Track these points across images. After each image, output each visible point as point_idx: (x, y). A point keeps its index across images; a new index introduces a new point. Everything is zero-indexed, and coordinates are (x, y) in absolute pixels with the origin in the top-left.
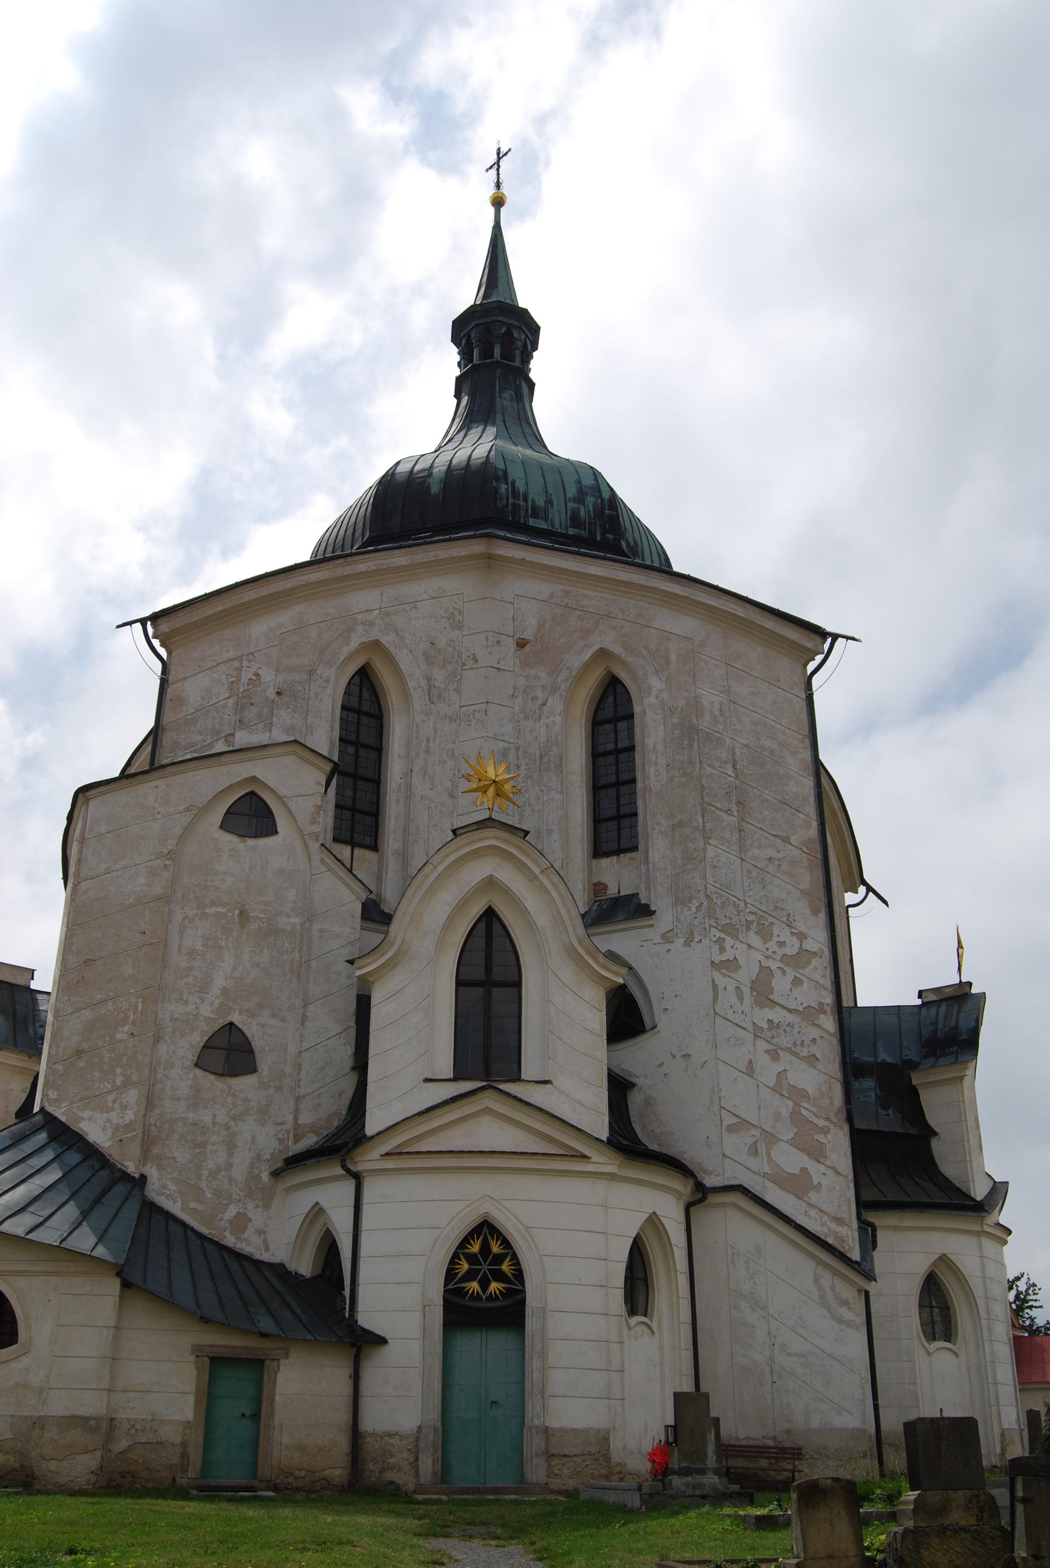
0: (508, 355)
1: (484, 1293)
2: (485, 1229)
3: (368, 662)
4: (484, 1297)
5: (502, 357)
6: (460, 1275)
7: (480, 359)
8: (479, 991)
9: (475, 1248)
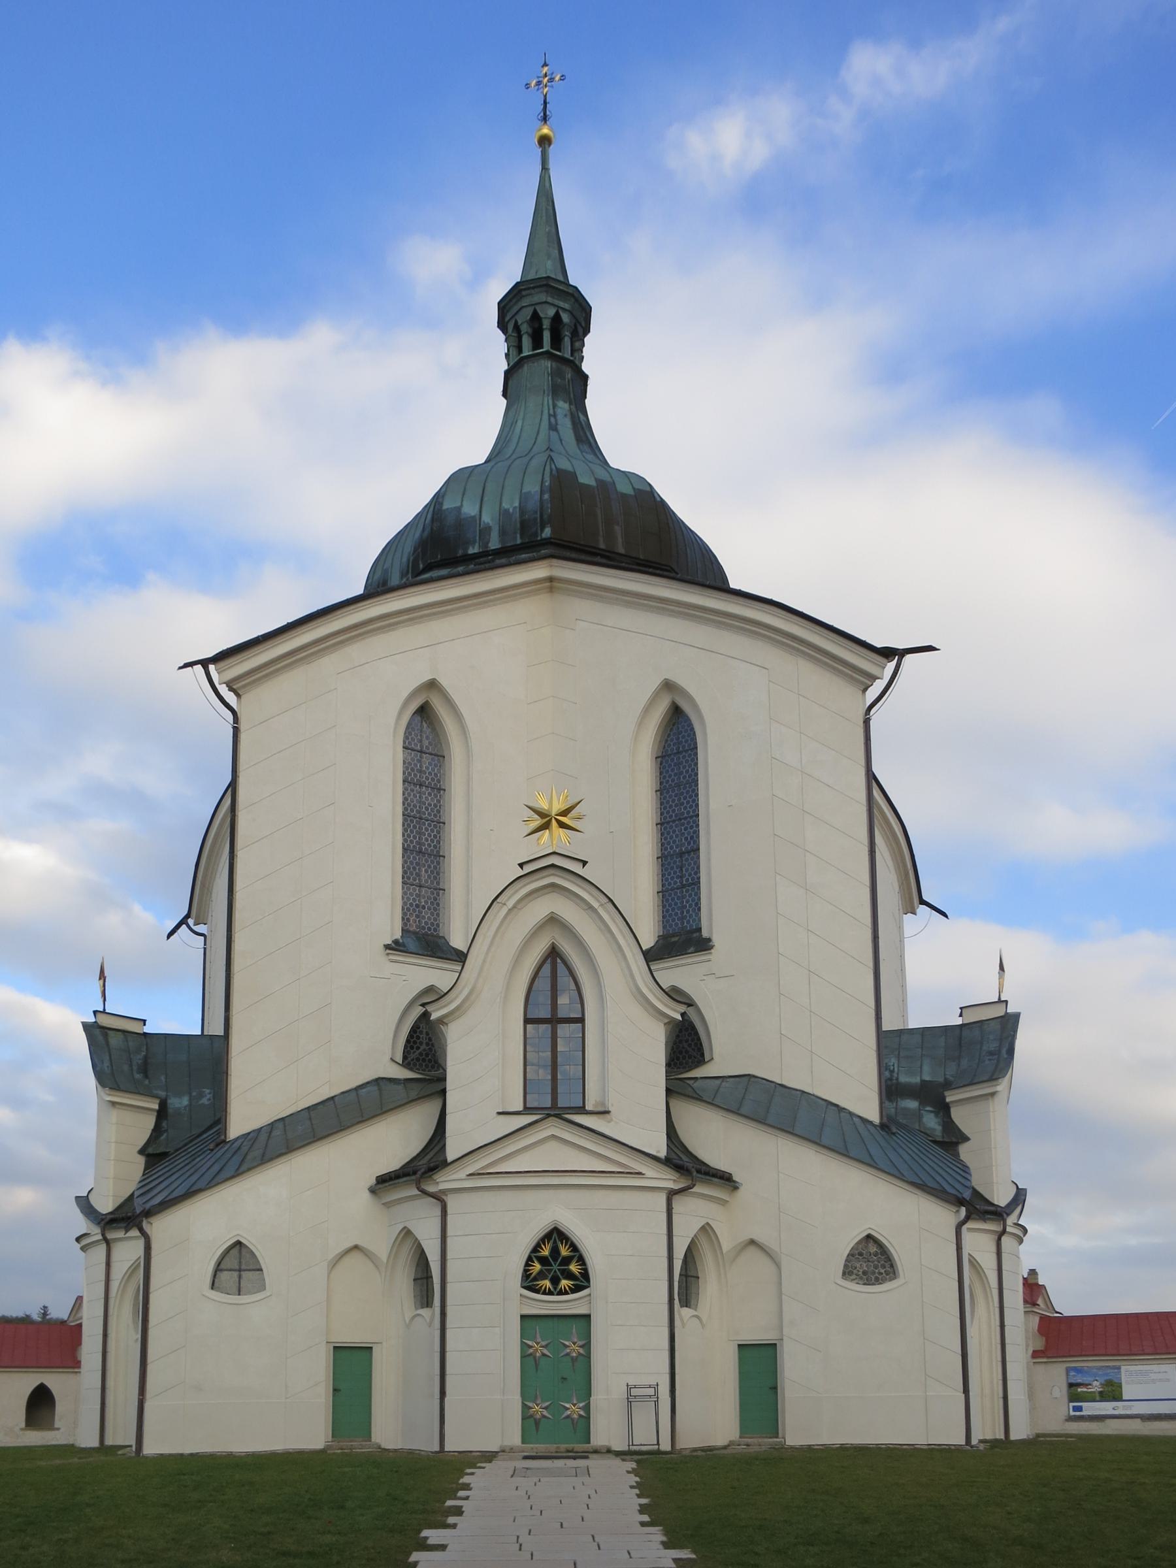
0: (556, 341)
1: (555, 1289)
2: (555, 1235)
6: (533, 1275)
8: (545, 1028)
9: (546, 1252)
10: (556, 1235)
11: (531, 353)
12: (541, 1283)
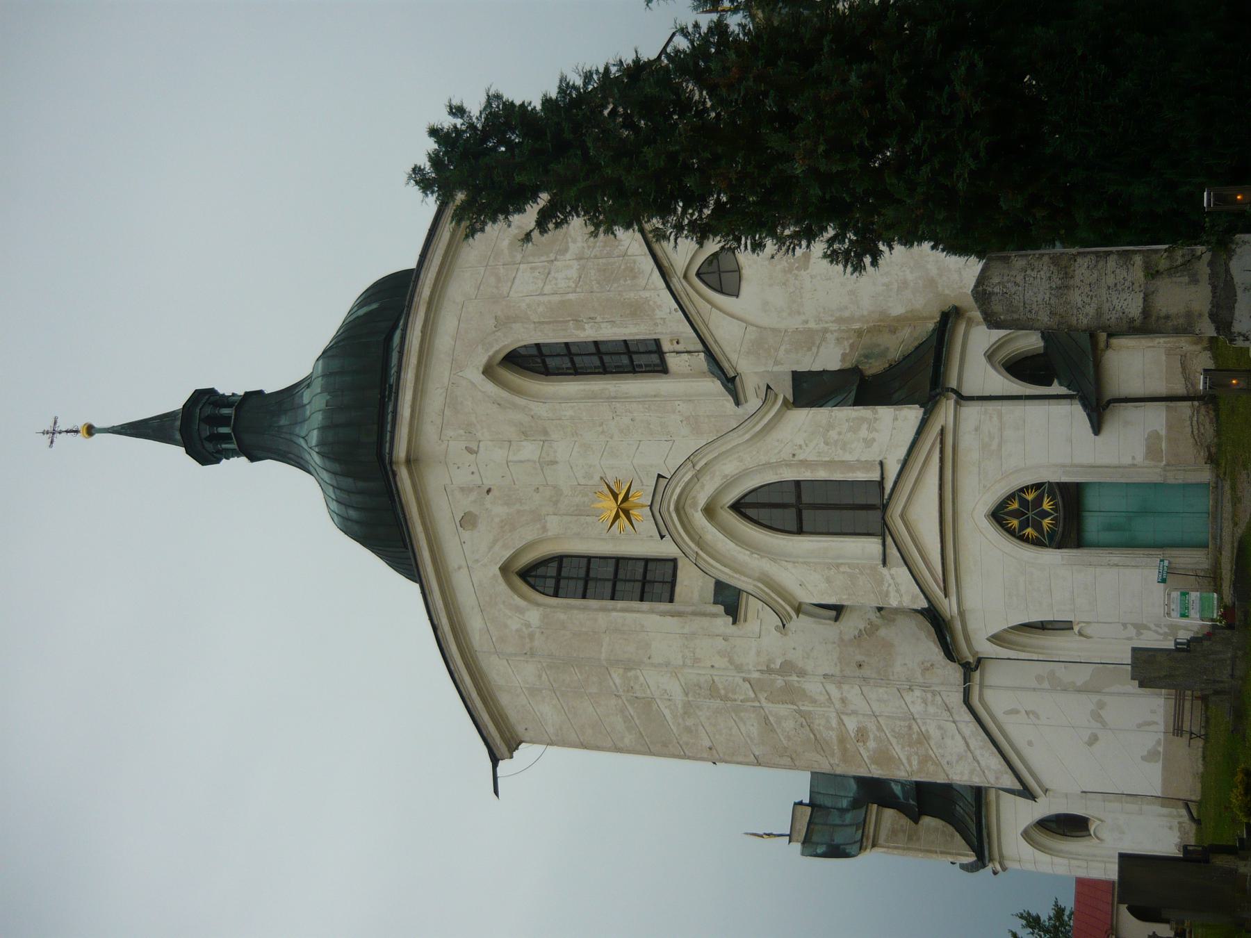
0: (225, 421)
3: (517, 573)
4: (1056, 514)
5: (227, 425)
7: (232, 443)
9: (1015, 523)
10: (998, 516)
11: (235, 442)
12: (1045, 527)
